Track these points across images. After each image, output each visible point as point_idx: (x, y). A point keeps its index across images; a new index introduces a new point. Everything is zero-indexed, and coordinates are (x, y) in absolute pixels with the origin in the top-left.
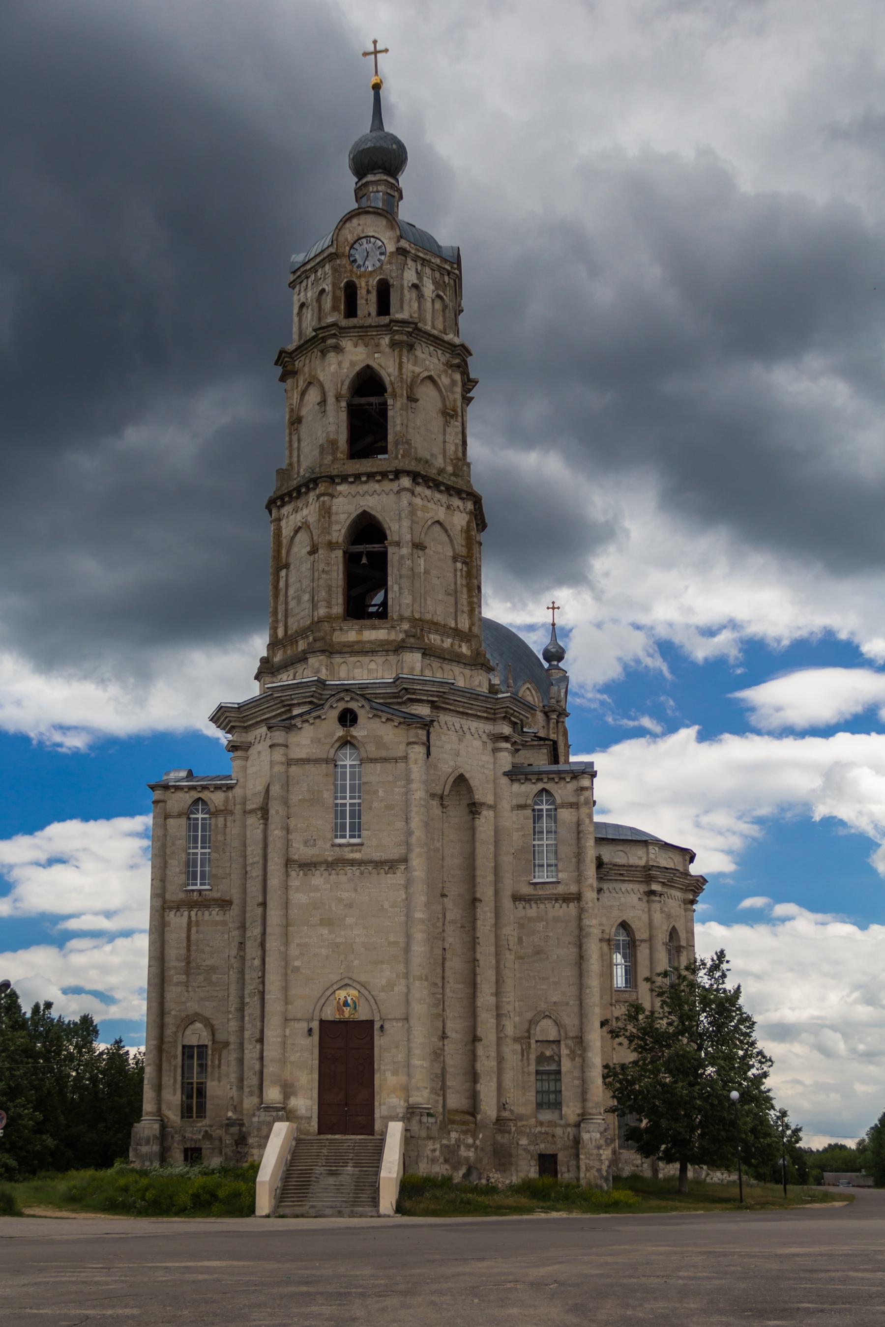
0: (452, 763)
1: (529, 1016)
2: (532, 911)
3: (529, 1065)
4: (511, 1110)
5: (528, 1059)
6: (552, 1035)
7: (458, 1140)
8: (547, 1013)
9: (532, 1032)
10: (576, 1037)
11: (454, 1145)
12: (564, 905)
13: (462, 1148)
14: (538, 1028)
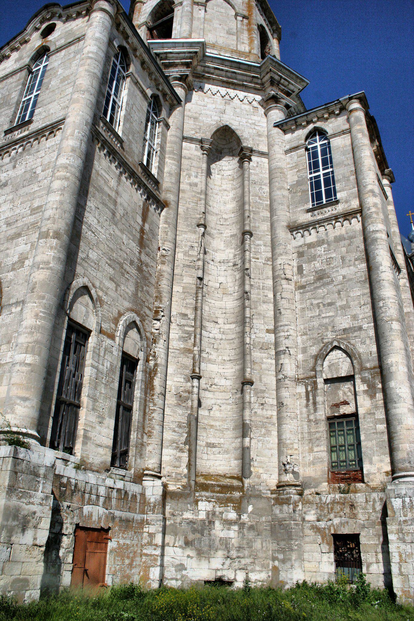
0: (217, 118)
1: (314, 350)
2: (311, 237)
3: (315, 410)
4: (293, 472)
5: (315, 403)
6: (344, 370)
7: (212, 515)
8: (335, 343)
9: (319, 368)
10: (375, 368)
11: (203, 521)
12: (346, 223)
13: (217, 523)
14: (326, 363)
